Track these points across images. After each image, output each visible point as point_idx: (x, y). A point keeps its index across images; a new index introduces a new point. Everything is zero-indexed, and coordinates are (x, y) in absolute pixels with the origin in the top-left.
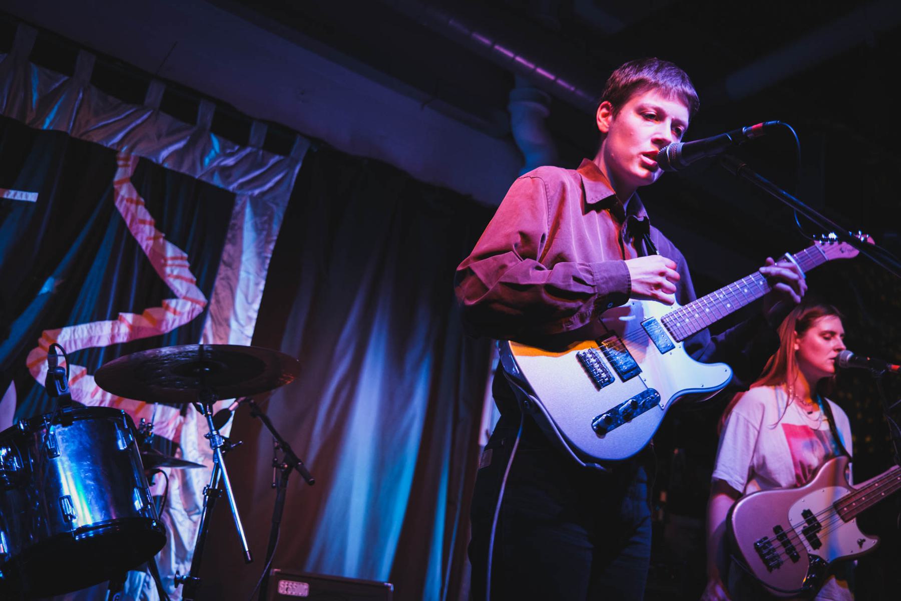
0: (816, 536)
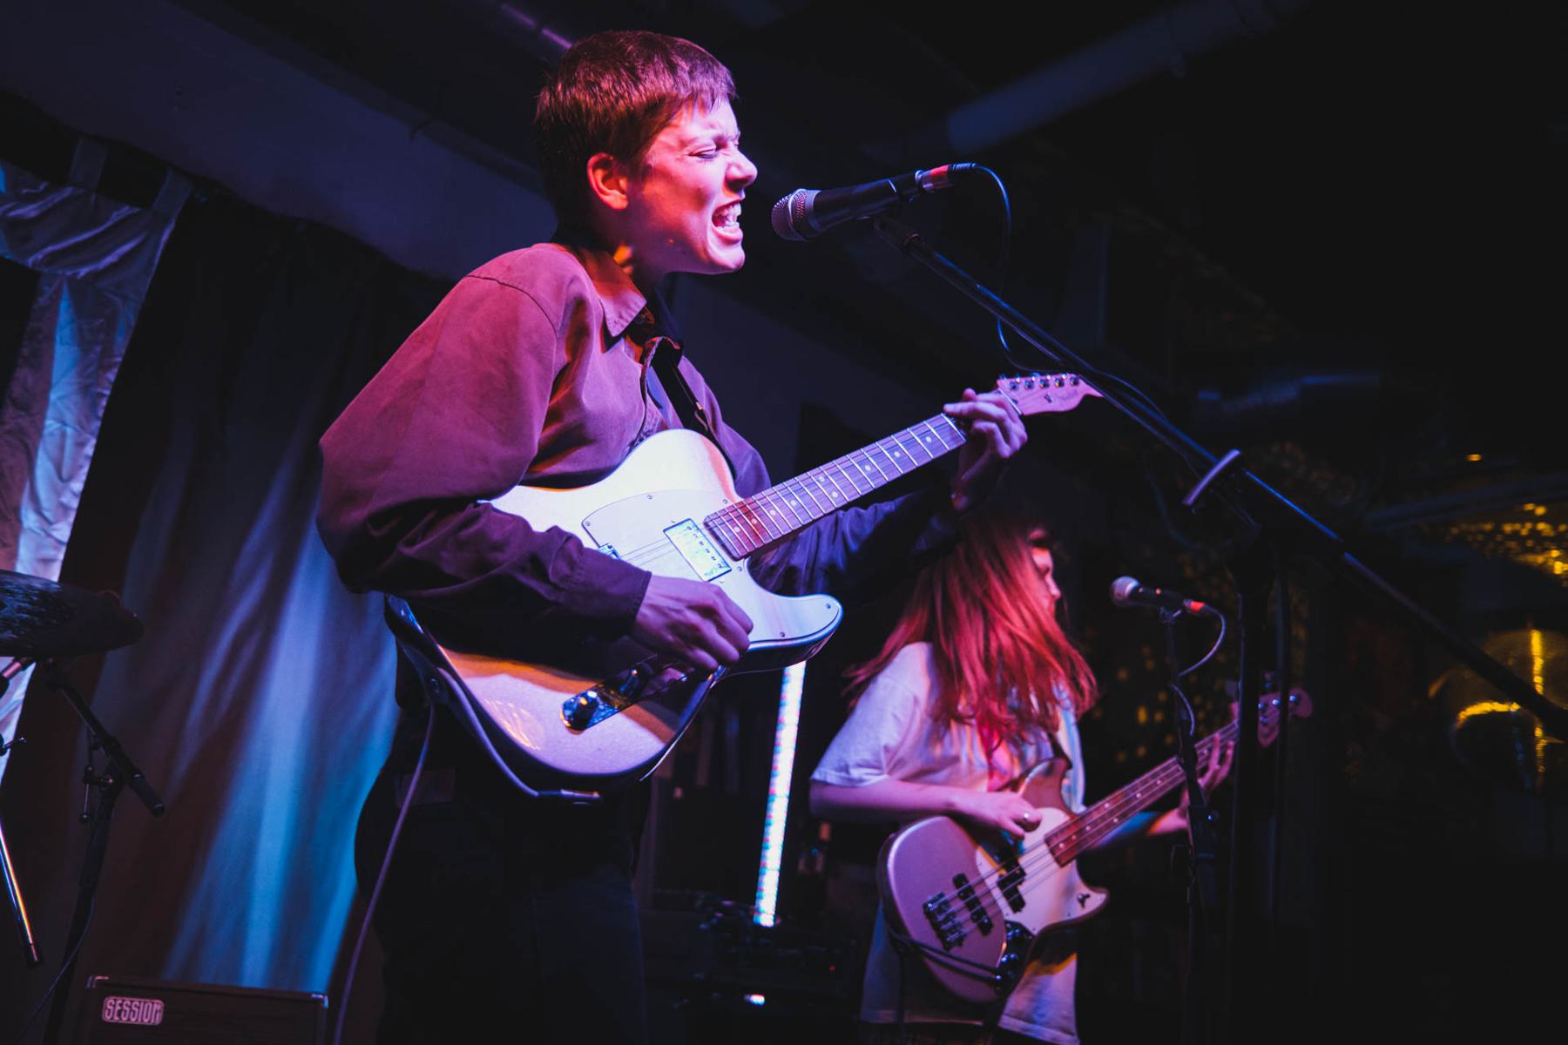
0: (1017, 891)
